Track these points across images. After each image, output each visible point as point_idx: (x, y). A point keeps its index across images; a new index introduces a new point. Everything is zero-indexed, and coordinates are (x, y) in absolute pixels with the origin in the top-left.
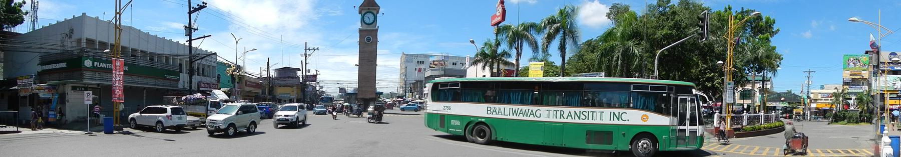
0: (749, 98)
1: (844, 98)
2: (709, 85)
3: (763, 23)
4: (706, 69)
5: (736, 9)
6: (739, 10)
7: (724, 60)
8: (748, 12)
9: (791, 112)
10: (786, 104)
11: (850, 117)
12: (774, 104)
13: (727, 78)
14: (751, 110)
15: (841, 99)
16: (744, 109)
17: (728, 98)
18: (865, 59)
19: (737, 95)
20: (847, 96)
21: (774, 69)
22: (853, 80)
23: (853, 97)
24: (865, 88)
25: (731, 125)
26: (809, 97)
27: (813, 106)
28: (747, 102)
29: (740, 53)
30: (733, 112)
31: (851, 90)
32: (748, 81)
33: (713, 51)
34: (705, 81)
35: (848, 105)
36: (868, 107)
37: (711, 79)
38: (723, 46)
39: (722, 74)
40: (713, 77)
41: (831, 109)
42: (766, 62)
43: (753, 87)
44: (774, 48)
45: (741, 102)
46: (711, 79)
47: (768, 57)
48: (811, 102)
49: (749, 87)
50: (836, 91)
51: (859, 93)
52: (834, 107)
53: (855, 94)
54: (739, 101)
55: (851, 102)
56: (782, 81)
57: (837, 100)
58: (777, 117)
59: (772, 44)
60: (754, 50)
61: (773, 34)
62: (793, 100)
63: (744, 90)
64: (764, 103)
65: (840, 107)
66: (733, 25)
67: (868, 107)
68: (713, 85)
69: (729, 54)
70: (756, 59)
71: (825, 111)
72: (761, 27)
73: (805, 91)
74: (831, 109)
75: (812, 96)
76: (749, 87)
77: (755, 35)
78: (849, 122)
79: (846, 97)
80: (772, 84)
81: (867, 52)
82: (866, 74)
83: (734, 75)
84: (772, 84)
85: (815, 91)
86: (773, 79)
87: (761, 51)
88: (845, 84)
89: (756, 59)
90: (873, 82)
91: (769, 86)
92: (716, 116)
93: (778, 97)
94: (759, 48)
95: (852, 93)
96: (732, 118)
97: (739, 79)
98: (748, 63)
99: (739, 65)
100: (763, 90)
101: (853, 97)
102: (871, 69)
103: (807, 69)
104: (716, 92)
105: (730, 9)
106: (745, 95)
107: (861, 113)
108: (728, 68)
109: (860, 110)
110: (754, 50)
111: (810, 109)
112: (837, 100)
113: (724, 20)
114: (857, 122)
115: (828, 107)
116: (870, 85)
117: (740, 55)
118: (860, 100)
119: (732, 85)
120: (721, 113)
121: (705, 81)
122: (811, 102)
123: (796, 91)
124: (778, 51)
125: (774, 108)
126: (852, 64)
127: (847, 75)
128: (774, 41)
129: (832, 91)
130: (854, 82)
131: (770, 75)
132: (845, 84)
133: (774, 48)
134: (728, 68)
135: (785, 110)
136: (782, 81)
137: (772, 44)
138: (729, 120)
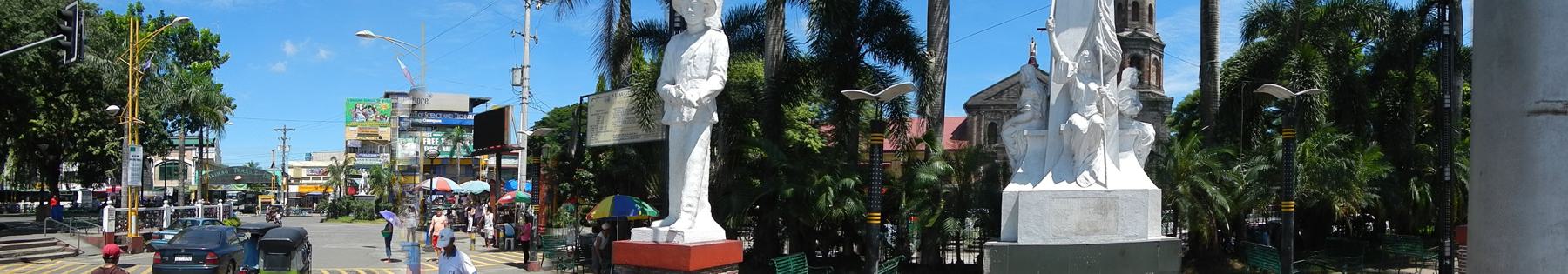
0: (176, 177)
1: (348, 176)
2: (96, 152)
3: (198, 42)
5: (151, 12)
6: (156, 16)
7: (123, 104)
8: (170, 20)
9: (255, 200)
10: (245, 188)
11: (360, 209)
12: (222, 188)
13: (128, 139)
14: (181, 201)
15: (342, 177)
16: (166, 197)
17: (131, 174)
18: (384, 106)
19: (155, 171)
20: (353, 172)
21: (219, 125)
22: (364, 143)
23: (365, 174)
24: (385, 157)
25: (138, 228)
26: (285, 174)
27: (294, 189)
28: (172, 185)
29: (155, 92)
30: (144, 202)
31: (360, 162)
32: (173, 146)
33: (99, 86)
34: (86, 145)
35: (356, 187)
36: (391, 192)
37: (99, 141)
38: (120, 77)
39: (120, 132)
40: (102, 136)
41: (325, 195)
42: (204, 113)
43: (182, 155)
44: (220, 87)
45: (161, 184)
46: (99, 141)
47: (207, 101)
48: (289, 183)
49: (173, 156)
50: (333, 163)
51: (374, 167)
52: (331, 191)
53: (367, 168)
54: (158, 183)
55: (361, 182)
56: (237, 145)
57: (336, 178)
58: (227, 211)
59: (216, 80)
60: (181, 88)
62: (257, 179)
63: (165, 163)
64: (203, 186)
65: (342, 191)
66: (137, 40)
67: (391, 192)
68: (103, 152)
69: (133, 92)
70: (186, 107)
71: (315, 198)
72: (195, 49)
73: (279, 163)
74: (325, 195)
75: (290, 172)
76: (173, 156)
77: (185, 62)
78: (357, 218)
79: (351, 173)
80: (218, 152)
81: (387, 95)
82: (386, 133)
83: (143, 135)
84: (218, 152)
85: (296, 164)
86: (222, 144)
88: (350, 150)
89: (186, 103)
90: (399, 147)
91: (212, 156)
92: (106, 211)
93: (230, 175)
94: (190, 86)
95: (362, 167)
96: (141, 215)
97: (153, 141)
98: (170, 112)
99: (152, 114)
100: (201, 163)
101: (365, 174)
102: (395, 124)
103: (282, 126)
104: (98, 168)
105: (140, 10)
106: (168, 171)
107: (378, 201)
108: (130, 121)
109: (377, 196)
110: (181, 88)
111: (287, 195)
112: (336, 178)
113: (121, 31)
114: (371, 219)
115: (320, 192)
116: (393, 153)
117: (155, 97)
118: (376, 179)
119: (140, 151)
120: (118, 205)
121: (86, 145)
122: (289, 183)
123: (265, 165)
124: (227, 92)
125: (224, 195)
126: (361, 116)
127: (352, 135)
128: (218, 76)
129: (327, 164)
130: (365, 147)
131: (212, 135)
132: (350, 150)
133: (220, 87)
134: (130, 121)
135: (243, 198)
136: (237, 145)
137: (216, 80)
138: (133, 219)
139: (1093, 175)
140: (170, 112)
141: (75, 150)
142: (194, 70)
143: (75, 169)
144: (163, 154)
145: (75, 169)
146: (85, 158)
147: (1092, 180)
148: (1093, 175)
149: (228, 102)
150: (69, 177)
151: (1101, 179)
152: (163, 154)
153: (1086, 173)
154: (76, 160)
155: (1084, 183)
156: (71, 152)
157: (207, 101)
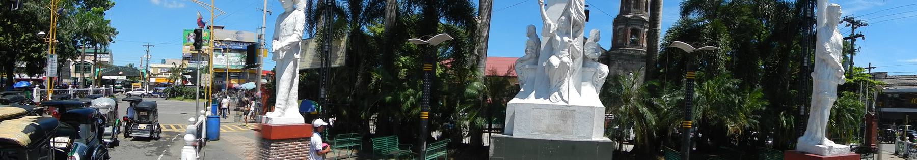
2: (36, 56)
4: (30, 38)
34: (30, 52)
37: (35, 50)
40: (40, 47)
42: (99, 36)
44: (108, 22)
46: (37, 50)
47: (99, 30)
59: (106, 18)
61: (107, 7)
68: (40, 57)
70: (85, 33)
87: (90, 24)
98: (78, 35)
121: (30, 52)
124: (111, 25)
128: (109, 15)
133: (108, 22)
137: (106, 18)
139: (561, 95)
140: (78, 35)
141: (23, 55)
142: (93, 12)
143: (24, 65)
144: (74, 58)
145: (24, 65)
146: (29, 59)
147: (559, 98)
148: (561, 95)
149: (113, 31)
150: (20, 70)
151: (565, 98)
152: (74, 58)
153: (556, 94)
154: (24, 60)
155: (555, 100)
156: (21, 55)
157: (99, 30)
